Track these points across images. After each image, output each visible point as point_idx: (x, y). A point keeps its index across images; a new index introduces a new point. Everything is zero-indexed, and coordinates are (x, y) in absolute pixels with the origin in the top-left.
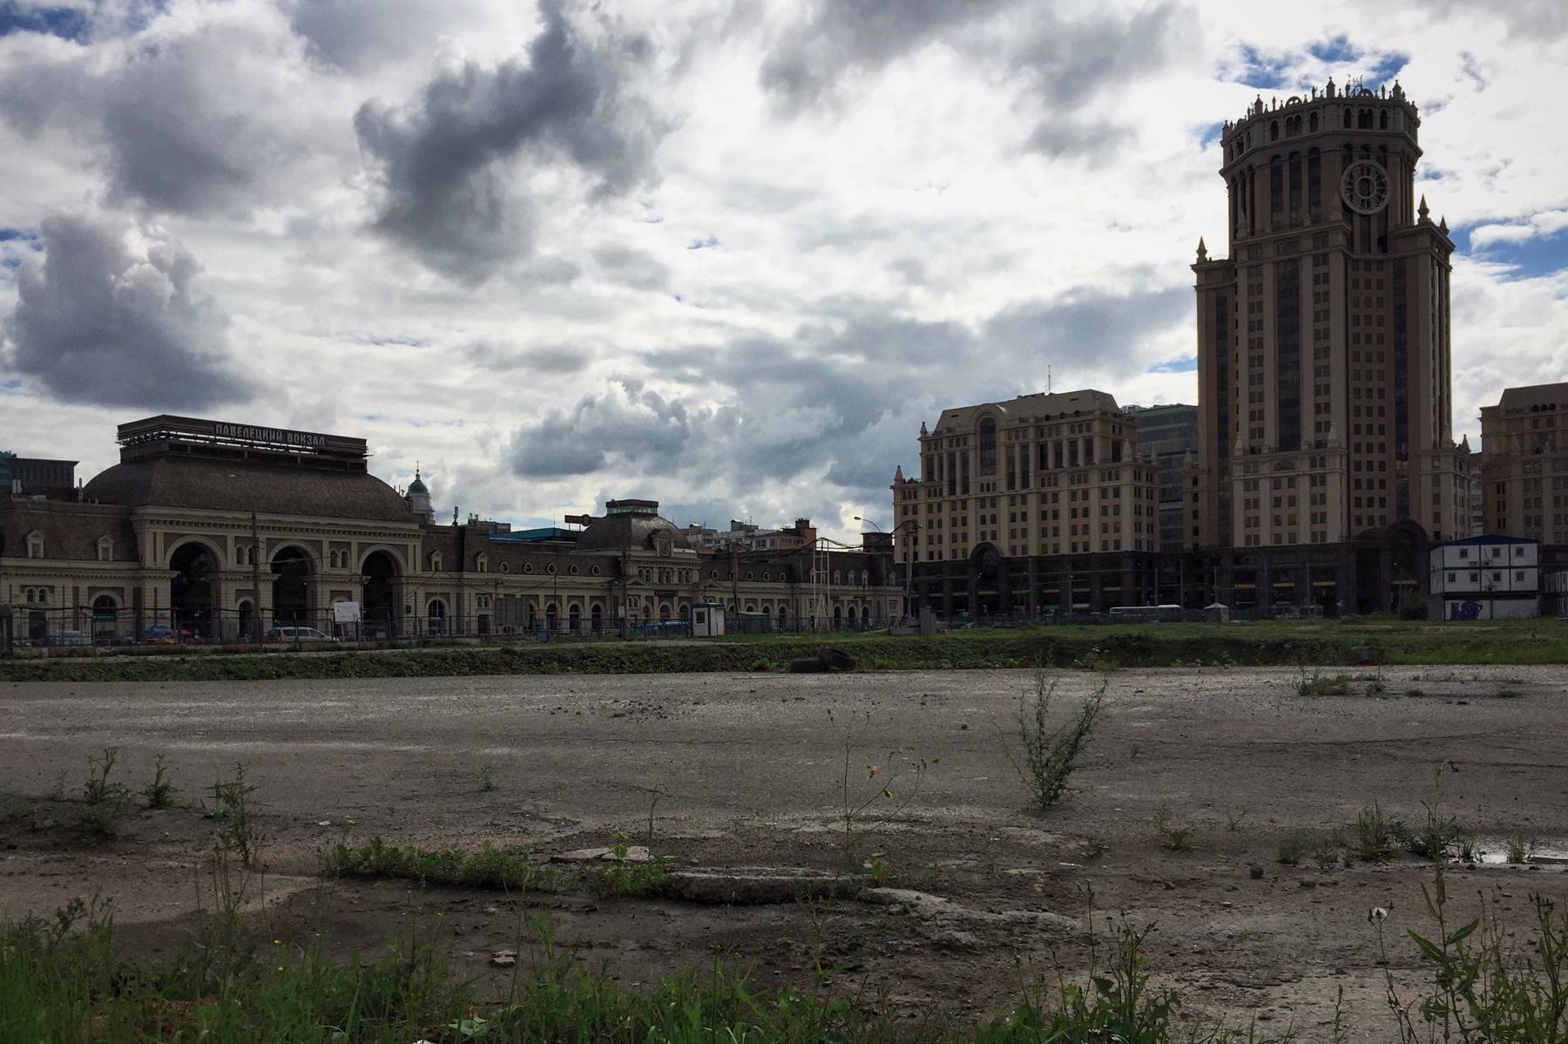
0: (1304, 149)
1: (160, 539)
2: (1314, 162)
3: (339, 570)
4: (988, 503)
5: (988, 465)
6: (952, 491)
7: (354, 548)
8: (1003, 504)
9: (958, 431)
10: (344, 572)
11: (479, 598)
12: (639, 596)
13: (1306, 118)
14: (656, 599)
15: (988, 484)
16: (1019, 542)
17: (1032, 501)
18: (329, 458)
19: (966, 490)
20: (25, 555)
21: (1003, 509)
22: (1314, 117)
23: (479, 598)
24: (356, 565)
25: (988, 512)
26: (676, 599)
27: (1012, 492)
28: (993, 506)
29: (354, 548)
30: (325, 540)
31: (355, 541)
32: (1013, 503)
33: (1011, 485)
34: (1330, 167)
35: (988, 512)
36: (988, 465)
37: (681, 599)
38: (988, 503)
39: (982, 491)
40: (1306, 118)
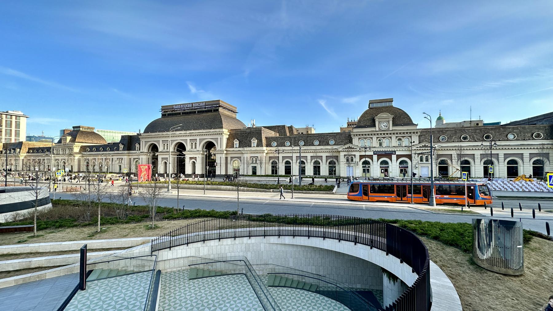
1: (144, 143)
3: (194, 149)
7: (198, 141)
10: (195, 150)
11: (253, 159)
12: (355, 155)
14: (375, 157)
18: (206, 109)
20: (119, 150)
23: (253, 159)
24: (200, 147)
26: (394, 157)
29: (198, 141)
30: (188, 138)
31: (198, 138)
37: (398, 157)
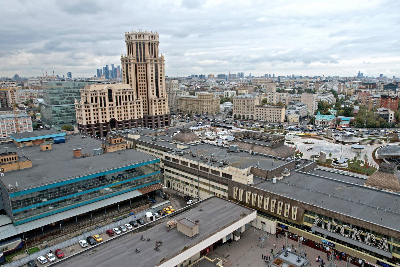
0: (142, 42)
2: (144, 45)
4: (111, 109)
5: (111, 100)
6: (101, 106)
8: (116, 110)
9: (102, 92)
13: (142, 36)
15: (111, 105)
16: (120, 117)
17: (122, 108)
19: (105, 105)
21: (116, 110)
22: (143, 36)
25: (112, 111)
27: (117, 106)
28: (113, 109)
32: (118, 108)
33: (117, 105)
34: (147, 47)
35: (112, 111)
36: (111, 100)
38: (111, 109)
39: (110, 106)
40: (142, 36)
